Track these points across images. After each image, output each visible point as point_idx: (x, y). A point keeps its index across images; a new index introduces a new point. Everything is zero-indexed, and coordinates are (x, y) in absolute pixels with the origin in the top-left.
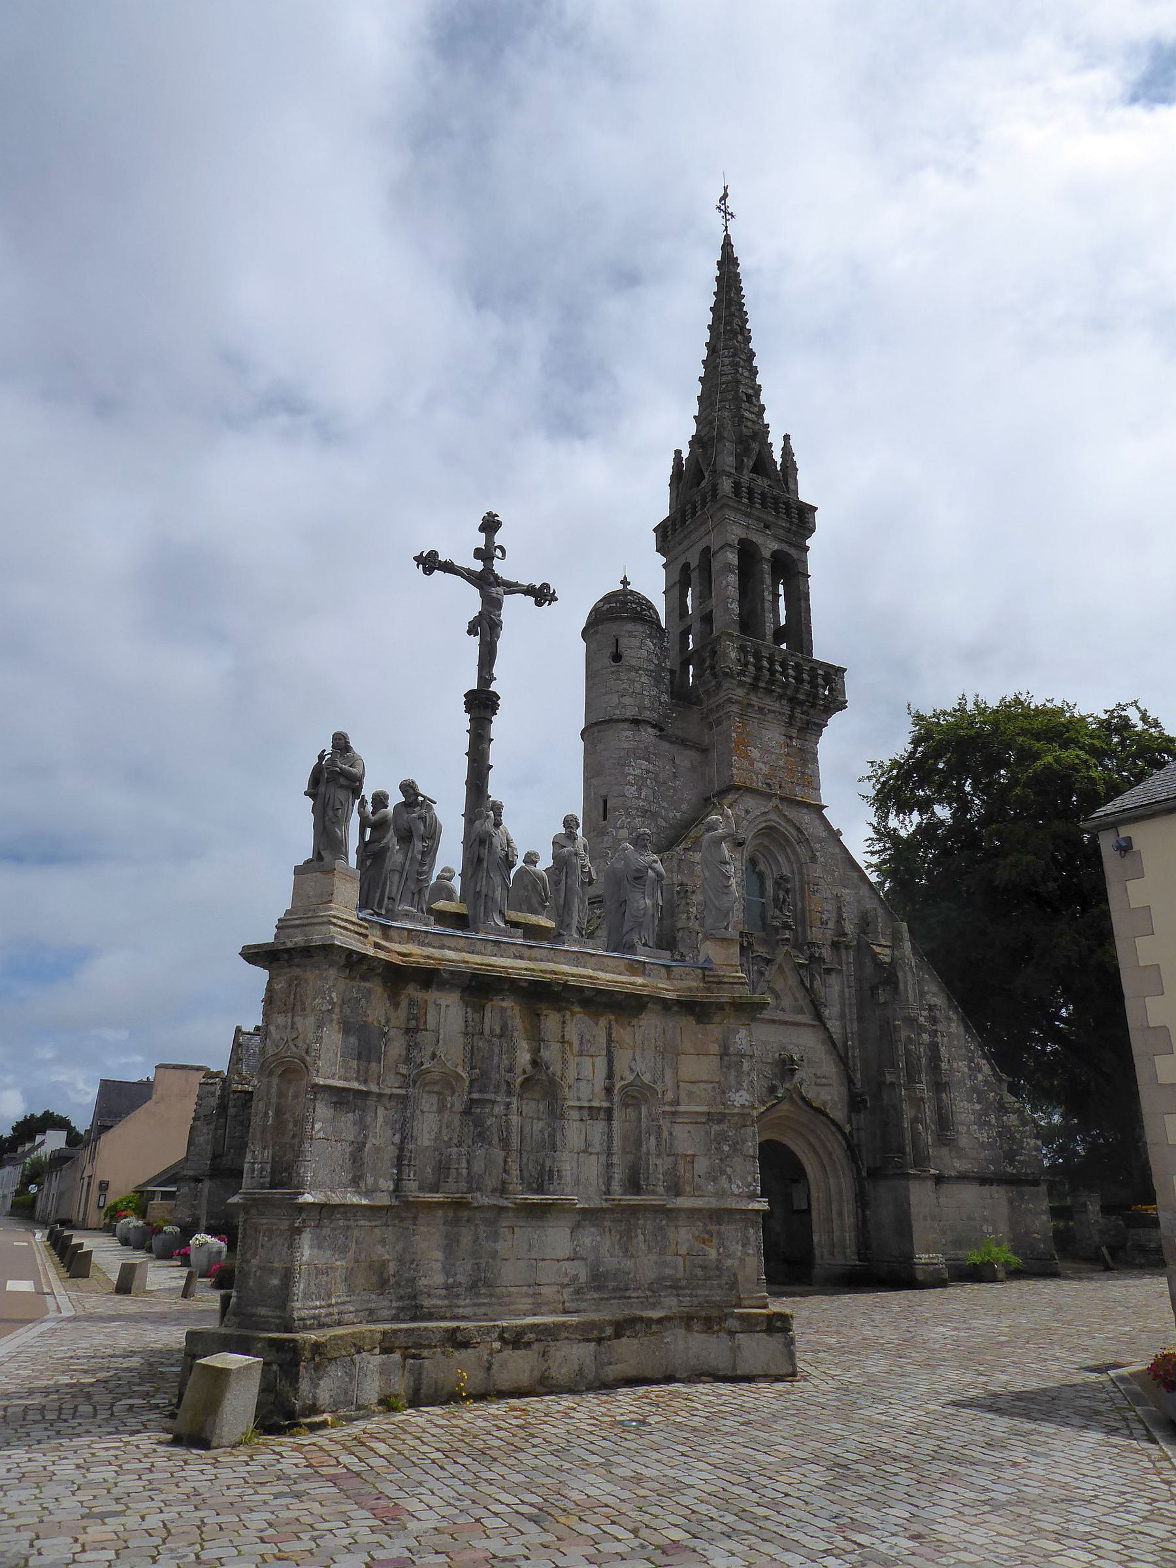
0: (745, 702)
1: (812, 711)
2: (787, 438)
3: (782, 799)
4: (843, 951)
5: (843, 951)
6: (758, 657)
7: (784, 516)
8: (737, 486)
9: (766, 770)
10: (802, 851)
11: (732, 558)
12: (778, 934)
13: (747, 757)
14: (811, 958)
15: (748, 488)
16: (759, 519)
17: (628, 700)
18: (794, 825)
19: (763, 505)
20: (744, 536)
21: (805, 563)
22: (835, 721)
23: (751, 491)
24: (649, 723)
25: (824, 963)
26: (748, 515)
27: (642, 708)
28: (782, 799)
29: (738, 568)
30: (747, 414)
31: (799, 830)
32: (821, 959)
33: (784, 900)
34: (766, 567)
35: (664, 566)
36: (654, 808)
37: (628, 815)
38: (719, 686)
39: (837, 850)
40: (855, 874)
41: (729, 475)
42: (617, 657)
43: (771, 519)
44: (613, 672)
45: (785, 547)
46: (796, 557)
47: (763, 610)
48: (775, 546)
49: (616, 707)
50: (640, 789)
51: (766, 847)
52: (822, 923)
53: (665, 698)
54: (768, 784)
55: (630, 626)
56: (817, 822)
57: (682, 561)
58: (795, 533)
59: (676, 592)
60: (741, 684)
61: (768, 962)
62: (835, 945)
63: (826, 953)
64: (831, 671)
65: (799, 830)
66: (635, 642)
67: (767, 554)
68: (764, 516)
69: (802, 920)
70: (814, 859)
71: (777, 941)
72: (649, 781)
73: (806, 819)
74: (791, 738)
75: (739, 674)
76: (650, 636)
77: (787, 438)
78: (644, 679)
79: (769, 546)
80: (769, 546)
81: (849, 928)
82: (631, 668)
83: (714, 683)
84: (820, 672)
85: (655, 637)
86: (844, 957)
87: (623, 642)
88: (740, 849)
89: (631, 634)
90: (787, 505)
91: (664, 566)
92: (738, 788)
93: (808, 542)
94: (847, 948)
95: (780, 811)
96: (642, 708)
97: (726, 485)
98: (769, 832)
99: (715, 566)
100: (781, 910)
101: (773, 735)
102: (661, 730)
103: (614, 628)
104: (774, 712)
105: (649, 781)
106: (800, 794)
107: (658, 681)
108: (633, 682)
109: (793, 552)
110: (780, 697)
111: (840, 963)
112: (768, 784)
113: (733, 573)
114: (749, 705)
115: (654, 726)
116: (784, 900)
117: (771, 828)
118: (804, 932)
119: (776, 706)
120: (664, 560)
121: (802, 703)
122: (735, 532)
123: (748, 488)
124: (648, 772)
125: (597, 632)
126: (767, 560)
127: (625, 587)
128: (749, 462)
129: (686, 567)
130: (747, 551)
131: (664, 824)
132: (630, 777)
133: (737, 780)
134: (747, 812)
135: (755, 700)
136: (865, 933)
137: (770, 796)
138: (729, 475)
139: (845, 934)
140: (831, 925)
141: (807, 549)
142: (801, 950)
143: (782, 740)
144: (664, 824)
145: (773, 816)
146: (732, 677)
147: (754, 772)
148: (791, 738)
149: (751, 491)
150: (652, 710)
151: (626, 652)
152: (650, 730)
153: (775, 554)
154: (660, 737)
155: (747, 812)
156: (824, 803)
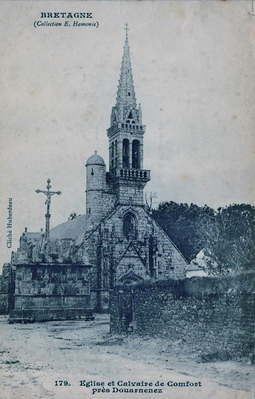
2: (140, 104)
8: (123, 125)
21: (142, 141)
23: (127, 126)
35: (109, 141)
45: (136, 138)
48: (134, 138)
57: (112, 141)
67: (131, 141)
77: (140, 104)
79: (131, 139)
80: (131, 139)
90: (137, 127)
109: (139, 139)
127: (96, 154)
128: (127, 116)
130: (126, 142)
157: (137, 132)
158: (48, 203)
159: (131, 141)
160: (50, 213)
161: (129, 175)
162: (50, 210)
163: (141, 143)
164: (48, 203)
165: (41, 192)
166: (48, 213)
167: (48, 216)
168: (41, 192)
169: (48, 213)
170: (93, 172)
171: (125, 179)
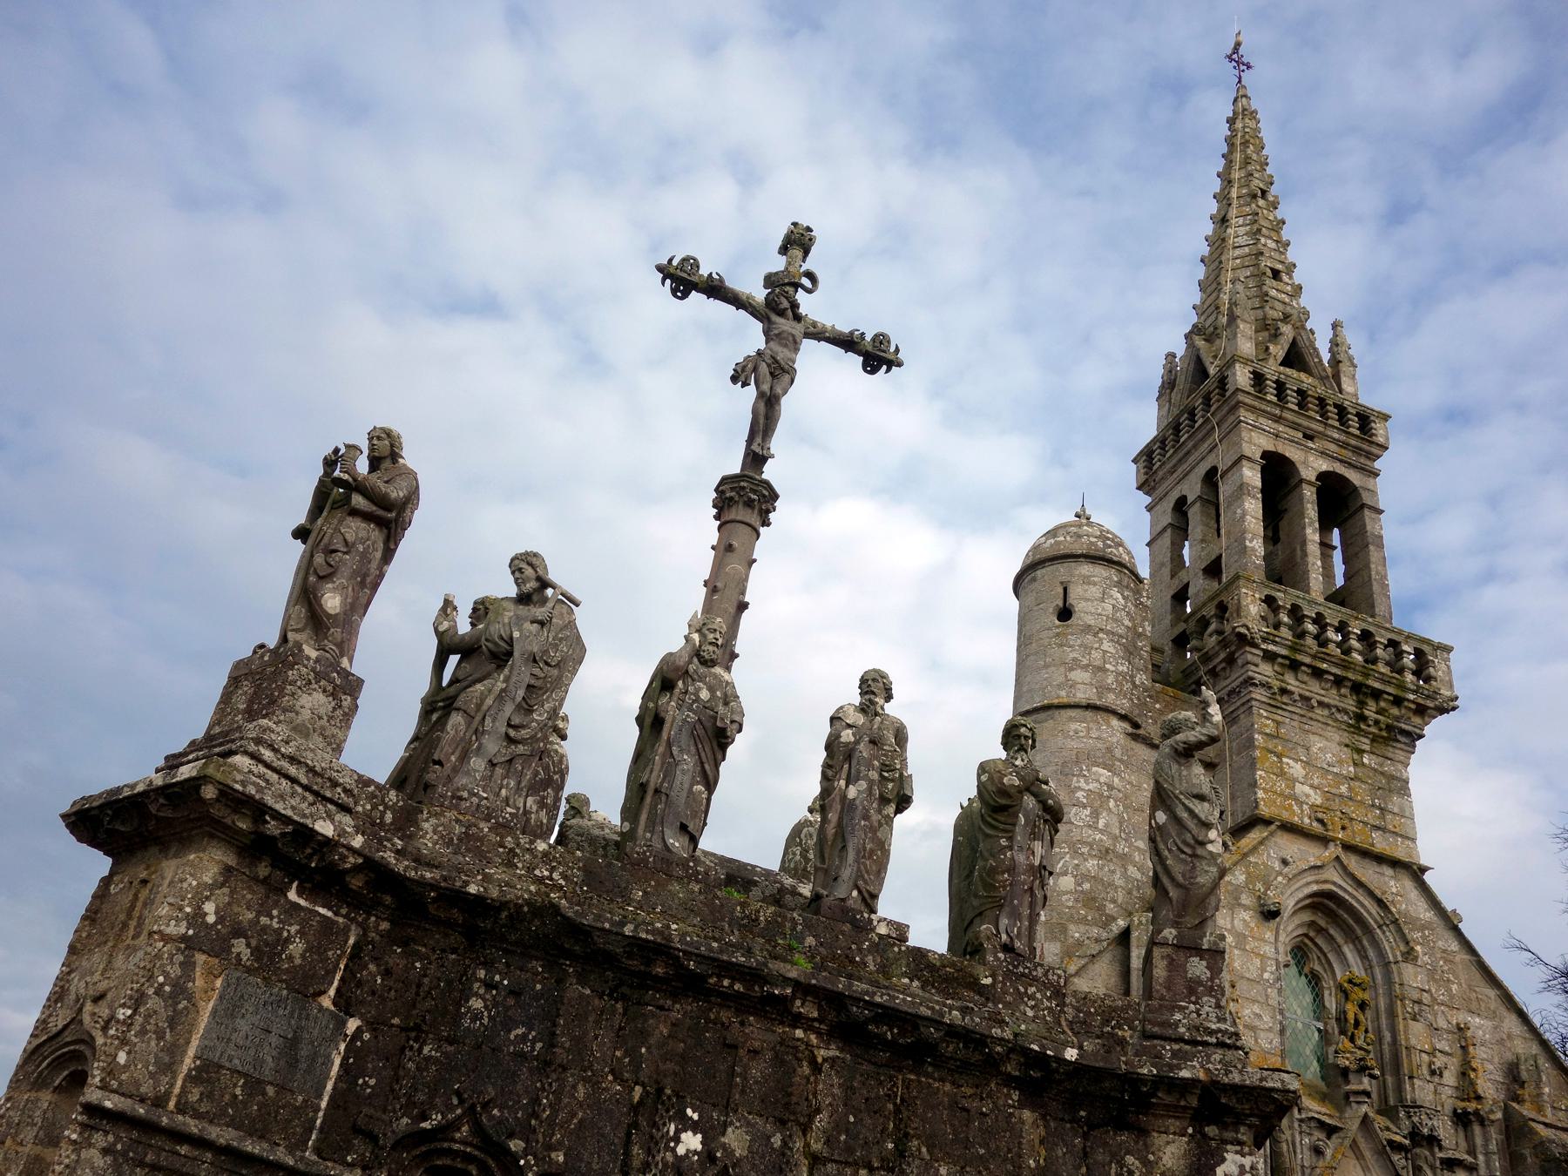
0: (1276, 684)
1: (1395, 711)
3: (1348, 847)
4: (1477, 1129)
5: (1477, 1129)
6: (1295, 611)
7: (1337, 424)
8: (1258, 379)
9: (1317, 798)
10: (1388, 940)
11: (1252, 476)
12: (1348, 1082)
13: (1282, 774)
14: (1414, 1135)
15: (1277, 382)
16: (1295, 426)
17: (1079, 675)
18: (1371, 894)
19: (1301, 405)
20: (1271, 448)
22: (1436, 728)
23: (1280, 387)
24: (1114, 712)
25: (1441, 1148)
26: (1278, 419)
27: (1102, 689)
28: (1348, 847)
29: (1263, 491)
30: (1273, 293)
31: (1380, 903)
32: (1433, 1141)
33: (1357, 1024)
34: (1309, 493)
35: (1150, 508)
36: (1121, 847)
37: (1075, 853)
38: (1231, 661)
39: (1454, 946)
40: (1492, 993)
41: (1246, 361)
42: (1065, 614)
43: (1314, 426)
44: (1058, 635)
46: (1357, 483)
47: (1305, 554)
48: (1324, 466)
49: (1059, 686)
50: (1095, 815)
51: (1321, 930)
52: (1433, 1073)
53: (1142, 678)
54: (1321, 821)
55: (1086, 569)
56: (1414, 894)
58: (1357, 450)
59: (1166, 540)
60: (1270, 657)
61: (1331, 1131)
62: (1462, 1120)
63: (1445, 1129)
64: (1425, 648)
65: (1380, 903)
66: (1094, 591)
67: (1309, 474)
68: (1305, 423)
69: (1395, 1063)
70: (1409, 955)
71: (1347, 1095)
72: (1112, 803)
73: (1393, 885)
74: (1360, 752)
75: (1264, 640)
76: (1119, 584)
78: (1107, 646)
79: (1311, 465)
81: (1489, 1085)
82: (1087, 629)
83: (1222, 656)
84: (1405, 648)
85: (1127, 587)
86: (1479, 1141)
87: (1076, 592)
88: (1273, 924)
89: (1087, 581)
90: (1342, 411)
91: (1150, 508)
92: (1267, 822)
93: (1377, 464)
94: (1482, 1122)
95: (1344, 868)
96: (1102, 689)
97: (1241, 377)
98: (1324, 904)
99: (1224, 490)
100: (1352, 1039)
101: (1328, 746)
102: (1136, 726)
103: (1061, 570)
104: (1328, 706)
105: (1112, 803)
106: (1380, 843)
107: (1130, 652)
108: (1087, 649)
110: (1339, 682)
111: (1472, 1151)
112: (1321, 821)
113: (1254, 497)
114: (1284, 691)
115: (1123, 718)
116: (1357, 1024)
117: (1330, 895)
118: (1399, 1089)
119: (1332, 697)
120: (1148, 500)
121: (1377, 695)
122: (1256, 439)
123: (1277, 382)
124: (1111, 787)
125: (1034, 579)
126: (1310, 483)
128: (1278, 350)
129: (1181, 506)
130: (1278, 473)
131: (1139, 876)
132: (1080, 794)
133: (1265, 810)
134: (1285, 862)
135: (1291, 682)
136: (1517, 1099)
137: (1324, 841)
138: (1246, 361)
139: (1479, 1098)
140: (1450, 1078)
141: (1376, 474)
142: (1394, 1118)
143: (1346, 754)
144: (1139, 876)
145: (1333, 875)
146: (1256, 646)
147: (1296, 799)
148: (1360, 752)
149: (1280, 387)
150: (1121, 693)
151: (1079, 606)
152: (1115, 722)
153: (1322, 476)
154: (1135, 737)
155: (1285, 862)
156: (1424, 862)
157: (1343, 438)
158: (767, 378)
159: (1309, 474)
160: (770, 472)
161: (1323, 643)
162: (777, 444)
163: (1366, 498)
164: (767, 378)
165: (716, 289)
166: (756, 459)
167: (745, 500)
168: (716, 289)
169: (756, 459)
170: (1070, 600)
171: (1294, 666)
